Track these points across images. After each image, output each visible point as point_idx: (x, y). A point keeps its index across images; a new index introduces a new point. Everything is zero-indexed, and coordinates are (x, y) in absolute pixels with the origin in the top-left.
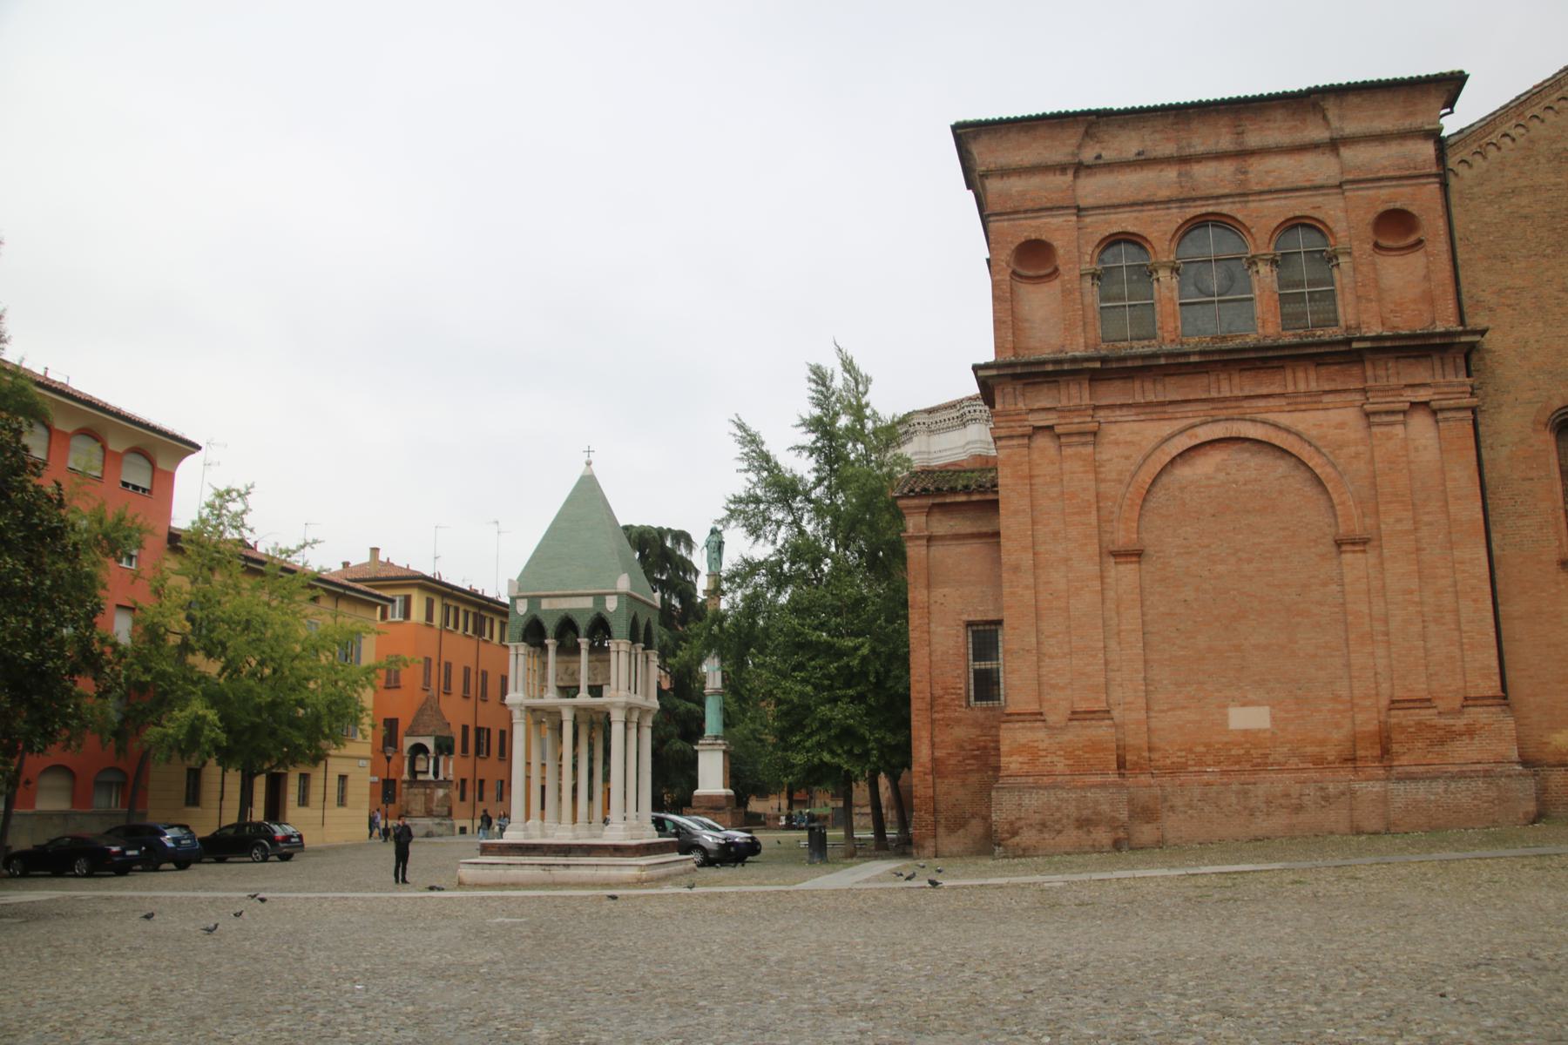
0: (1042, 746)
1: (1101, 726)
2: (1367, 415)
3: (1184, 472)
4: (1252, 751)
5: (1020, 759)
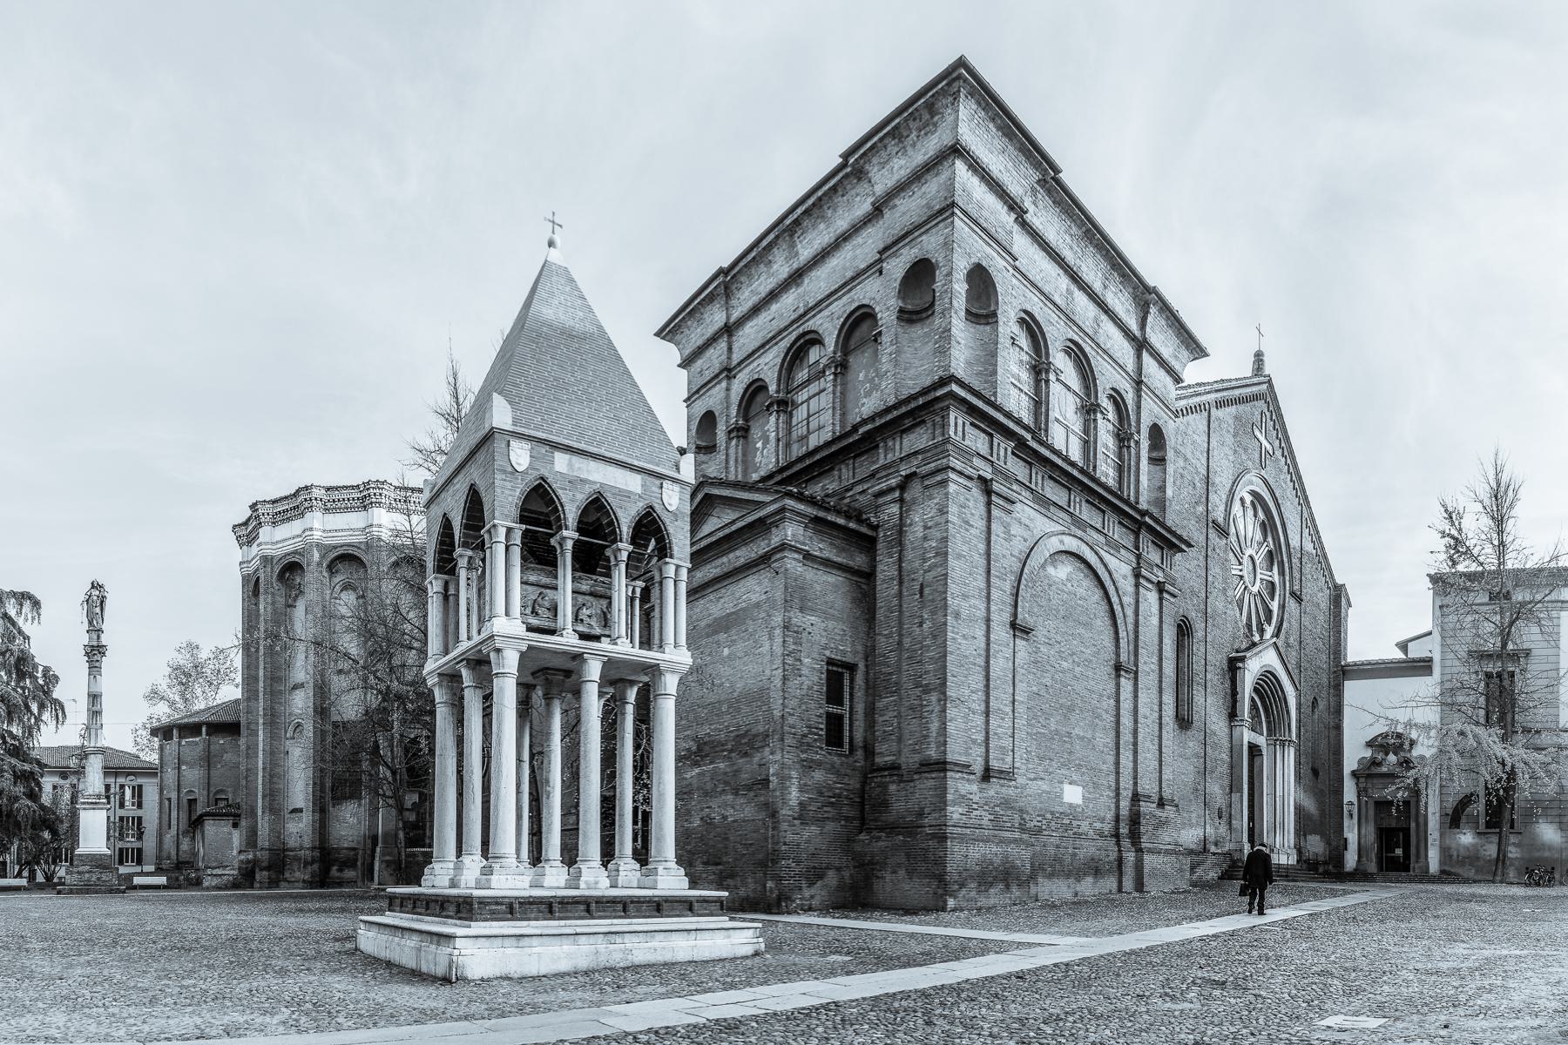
0: (976, 799)
3: (1050, 570)
5: (960, 810)
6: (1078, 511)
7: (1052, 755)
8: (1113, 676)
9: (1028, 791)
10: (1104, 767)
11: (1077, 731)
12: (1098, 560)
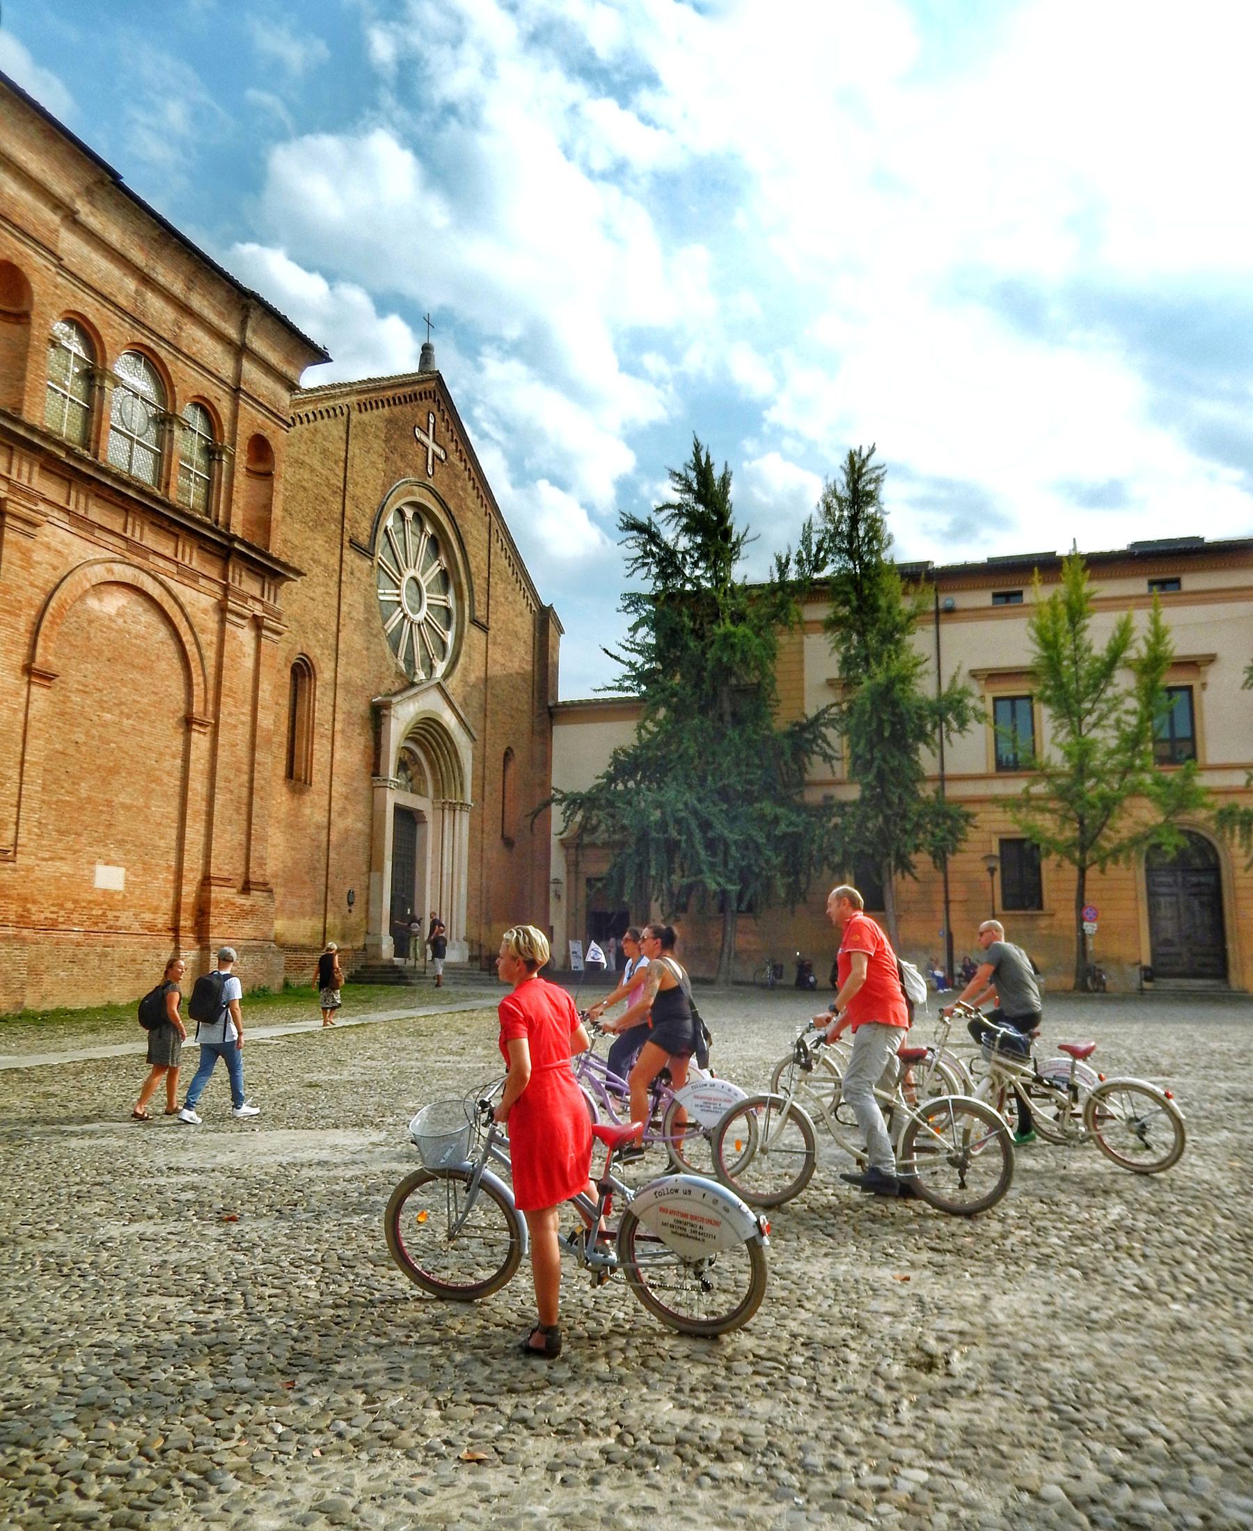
1: (5, 869)
2: (222, 609)
3: (92, 603)
4: (108, 913)
6: (137, 534)
7: (79, 828)
8: (181, 730)
9: (37, 874)
10: (162, 843)
11: (123, 798)
12: (164, 593)
